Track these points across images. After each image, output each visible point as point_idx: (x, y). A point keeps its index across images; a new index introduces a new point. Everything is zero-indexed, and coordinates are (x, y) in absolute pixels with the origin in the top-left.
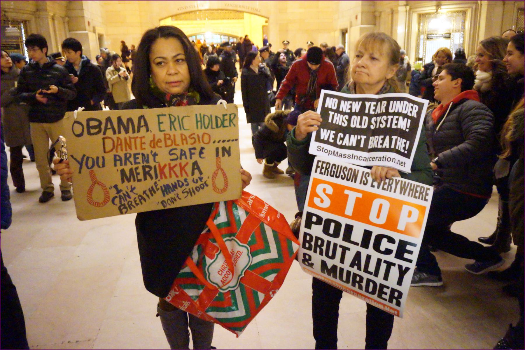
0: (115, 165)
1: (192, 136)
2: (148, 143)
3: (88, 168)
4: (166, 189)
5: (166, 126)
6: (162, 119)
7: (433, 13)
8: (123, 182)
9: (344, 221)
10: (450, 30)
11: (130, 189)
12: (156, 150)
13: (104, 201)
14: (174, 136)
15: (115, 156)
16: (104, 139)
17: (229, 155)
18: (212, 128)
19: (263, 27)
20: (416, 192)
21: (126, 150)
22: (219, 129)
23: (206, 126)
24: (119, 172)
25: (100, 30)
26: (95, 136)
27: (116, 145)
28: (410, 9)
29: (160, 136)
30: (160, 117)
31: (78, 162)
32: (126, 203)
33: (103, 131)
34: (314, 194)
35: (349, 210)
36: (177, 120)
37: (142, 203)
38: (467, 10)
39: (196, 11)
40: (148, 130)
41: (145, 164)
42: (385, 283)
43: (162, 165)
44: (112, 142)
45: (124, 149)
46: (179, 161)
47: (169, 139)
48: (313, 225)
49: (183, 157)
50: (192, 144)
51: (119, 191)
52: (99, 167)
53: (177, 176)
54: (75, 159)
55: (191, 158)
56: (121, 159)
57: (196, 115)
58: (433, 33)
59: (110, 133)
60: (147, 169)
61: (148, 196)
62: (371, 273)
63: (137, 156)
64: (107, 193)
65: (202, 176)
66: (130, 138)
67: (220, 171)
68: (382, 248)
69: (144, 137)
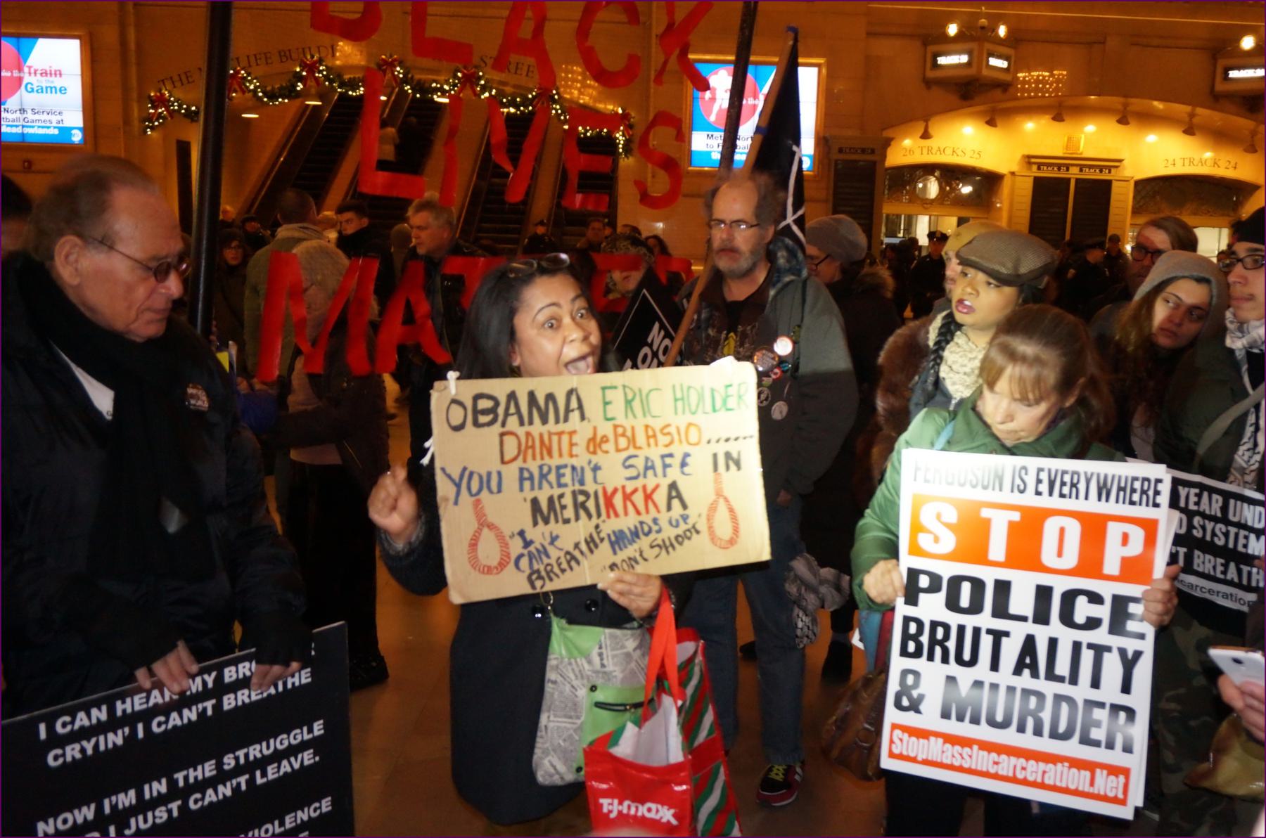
0: (521, 489)
1: (666, 431)
2: (583, 444)
3: (472, 495)
4: (617, 542)
5: (617, 409)
6: (610, 395)
8: (535, 524)
9: (990, 576)
11: (549, 540)
12: (598, 459)
14: (633, 428)
15: (521, 470)
17: (739, 468)
20: (1133, 491)
21: (542, 458)
23: (693, 409)
24: (528, 505)
26: (486, 429)
27: (523, 447)
29: (605, 429)
30: (608, 392)
32: (542, 568)
33: (500, 418)
34: (917, 528)
35: (997, 550)
37: (571, 568)
40: (583, 418)
41: (577, 487)
42: (1095, 695)
43: (610, 490)
45: (538, 456)
46: (638, 483)
47: (623, 435)
48: (922, 596)
51: (527, 544)
53: (638, 513)
54: (449, 476)
55: (665, 476)
56: (531, 478)
57: (674, 387)
59: (513, 422)
60: (581, 498)
61: (582, 553)
62: (1061, 679)
63: (562, 471)
64: (504, 545)
65: (687, 512)
66: (550, 434)
67: (721, 501)
68: (1080, 618)
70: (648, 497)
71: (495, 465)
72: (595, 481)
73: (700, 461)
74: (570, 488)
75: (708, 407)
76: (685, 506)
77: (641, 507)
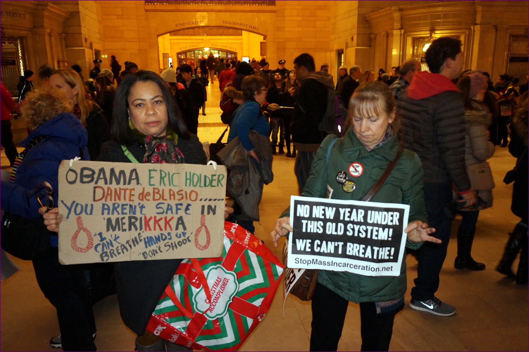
0: (103, 214)
4: (148, 242)
5: (156, 181)
8: (108, 230)
11: (114, 238)
12: (144, 202)
13: (87, 247)
14: (163, 190)
15: (104, 205)
16: (95, 188)
17: (214, 213)
18: (200, 186)
21: (115, 200)
22: (207, 188)
23: (195, 184)
24: (106, 221)
26: (87, 184)
27: (106, 194)
29: (149, 189)
30: (152, 172)
31: (67, 207)
32: (108, 251)
33: (95, 180)
36: (167, 176)
37: (123, 253)
40: (138, 183)
41: (132, 215)
43: (148, 218)
44: (102, 191)
46: (164, 215)
47: (158, 193)
49: (169, 212)
50: (179, 200)
51: (102, 239)
52: (87, 213)
53: (161, 229)
54: (65, 205)
55: (177, 213)
56: (108, 209)
57: (186, 173)
59: (101, 183)
61: (130, 246)
63: (125, 207)
66: (120, 189)
67: (203, 228)
69: (134, 189)
70: (167, 223)
71: (90, 201)
74: (128, 215)
75: (202, 184)
76: (185, 228)
77: (163, 227)
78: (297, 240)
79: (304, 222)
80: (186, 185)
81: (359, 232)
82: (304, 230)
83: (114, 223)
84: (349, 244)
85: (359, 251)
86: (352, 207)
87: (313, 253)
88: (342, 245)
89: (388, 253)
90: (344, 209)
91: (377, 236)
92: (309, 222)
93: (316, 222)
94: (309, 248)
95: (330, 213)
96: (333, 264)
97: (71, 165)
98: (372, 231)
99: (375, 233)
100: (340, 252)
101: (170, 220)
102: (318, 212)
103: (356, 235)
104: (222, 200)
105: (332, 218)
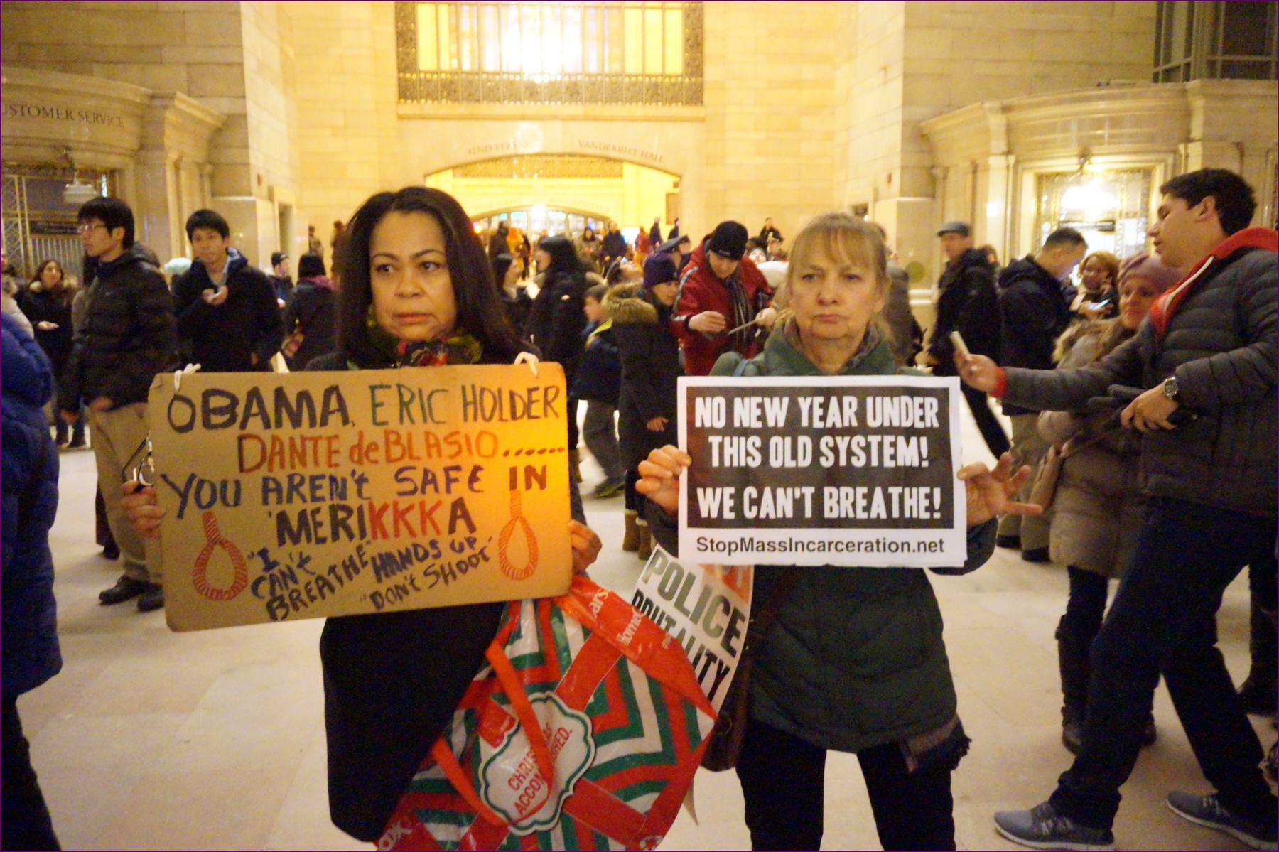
0: (265, 501)
2: (345, 452)
4: (383, 566)
5: (389, 412)
7: (1072, 173)
8: (281, 542)
10: (1113, 213)
11: (297, 560)
14: (410, 435)
15: (266, 480)
16: (241, 439)
18: (501, 419)
19: (668, 196)
21: (293, 467)
23: (488, 415)
24: (273, 522)
25: (285, 195)
26: (220, 431)
28: (1017, 162)
29: (374, 434)
30: (378, 393)
32: (286, 594)
33: (240, 419)
36: (417, 400)
37: (324, 598)
38: (1154, 168)
39: (509, 158)
40: (346, 421)
41: (337, 501)
43: (378, 506)
44: (260, 446)
47: (397, 442)
50: (452, 457)
51: (270, 565)
52: (225, 503)
53: (412, 533)
54: (172, 485)
55: (448, 491)
56: (278, 489)
57: (463, 388)
58: (1074, 218)
59: (255, 425)
60: (341, 515)
61: (339, 579)
63: (318, 482)
64: (241, 566)
65: (474, 535)
66: (303, 439)
67: (518, 524)
69: (336, 437)
70: (426, 516)
71: (233, 472)
72: (360, 494)
73: (495, 476)
77: (416, 526)
78: (700, 491)
79: (715, 440)
80: (466, 419)
81: (850, 453)
82: (715, 463)
83: (294, 523)
84: (827, 490)
85: (854, 505)
86: (827, 393)
87: (741, 522)
88: (813, 496)
89: (927, 503)
90: (809, 400)
91: (893, 457)
92: (727, 439)
93: (743, 439)
94: (732, 509)
95: (777, 412)
96: (793, 546)
97: (177, 385)
98: (881, 445)
99: (888, 451)
100: (808, 513)
101: (433, 509)
102: (746, 412)
103: (843, 462)
104: (561, 450)
105: (781, 424)
